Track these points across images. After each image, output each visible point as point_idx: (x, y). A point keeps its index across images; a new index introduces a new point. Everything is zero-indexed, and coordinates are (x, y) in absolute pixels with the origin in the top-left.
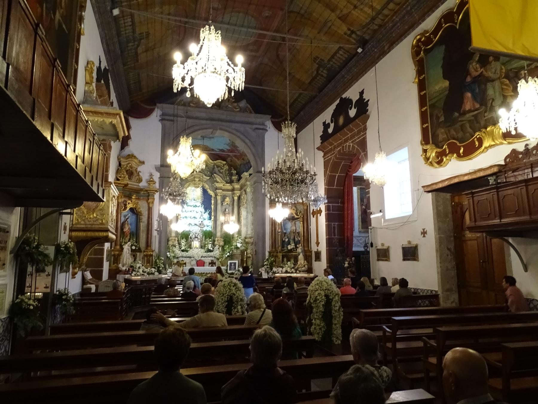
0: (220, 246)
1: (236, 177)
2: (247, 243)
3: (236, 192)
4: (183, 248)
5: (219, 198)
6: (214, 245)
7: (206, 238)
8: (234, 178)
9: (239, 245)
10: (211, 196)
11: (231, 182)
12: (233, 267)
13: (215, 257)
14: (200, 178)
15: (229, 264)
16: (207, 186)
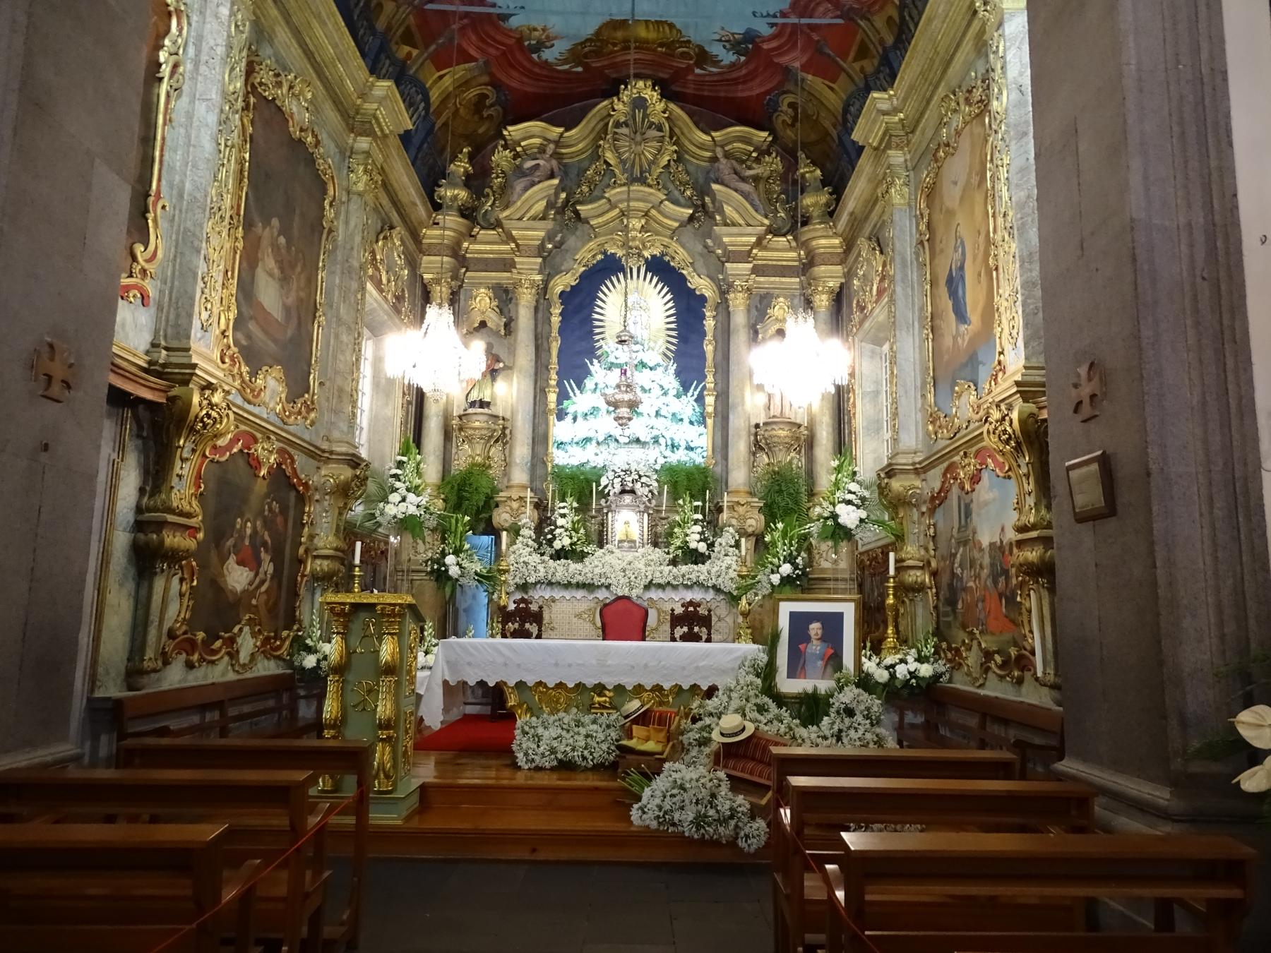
0: (742, 533)
1: (823, 198)
2: (895, 504)
3: (821, 270)
4: (563, 541)
5: (738, 302)
6: (712, 525)
7: (675, 495)
8: (813, 201)
9: (849, 516)
10: (703, 299)
11: (797, 223)
12: (815, 647)
13: (717, 589)
14: (646, 214)
15: (784, 623)
16: (680, 256)
